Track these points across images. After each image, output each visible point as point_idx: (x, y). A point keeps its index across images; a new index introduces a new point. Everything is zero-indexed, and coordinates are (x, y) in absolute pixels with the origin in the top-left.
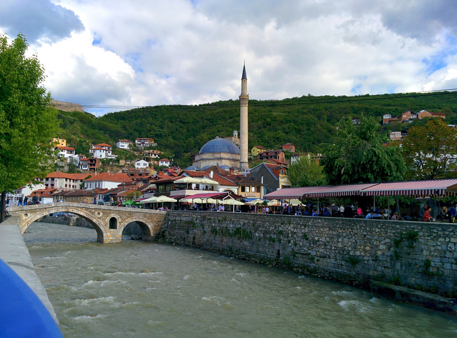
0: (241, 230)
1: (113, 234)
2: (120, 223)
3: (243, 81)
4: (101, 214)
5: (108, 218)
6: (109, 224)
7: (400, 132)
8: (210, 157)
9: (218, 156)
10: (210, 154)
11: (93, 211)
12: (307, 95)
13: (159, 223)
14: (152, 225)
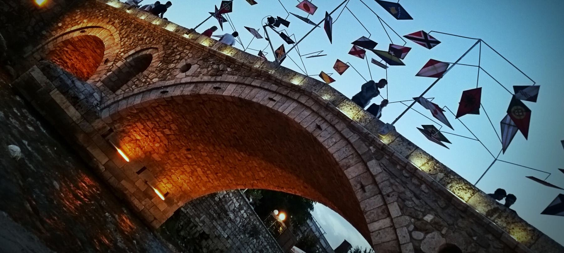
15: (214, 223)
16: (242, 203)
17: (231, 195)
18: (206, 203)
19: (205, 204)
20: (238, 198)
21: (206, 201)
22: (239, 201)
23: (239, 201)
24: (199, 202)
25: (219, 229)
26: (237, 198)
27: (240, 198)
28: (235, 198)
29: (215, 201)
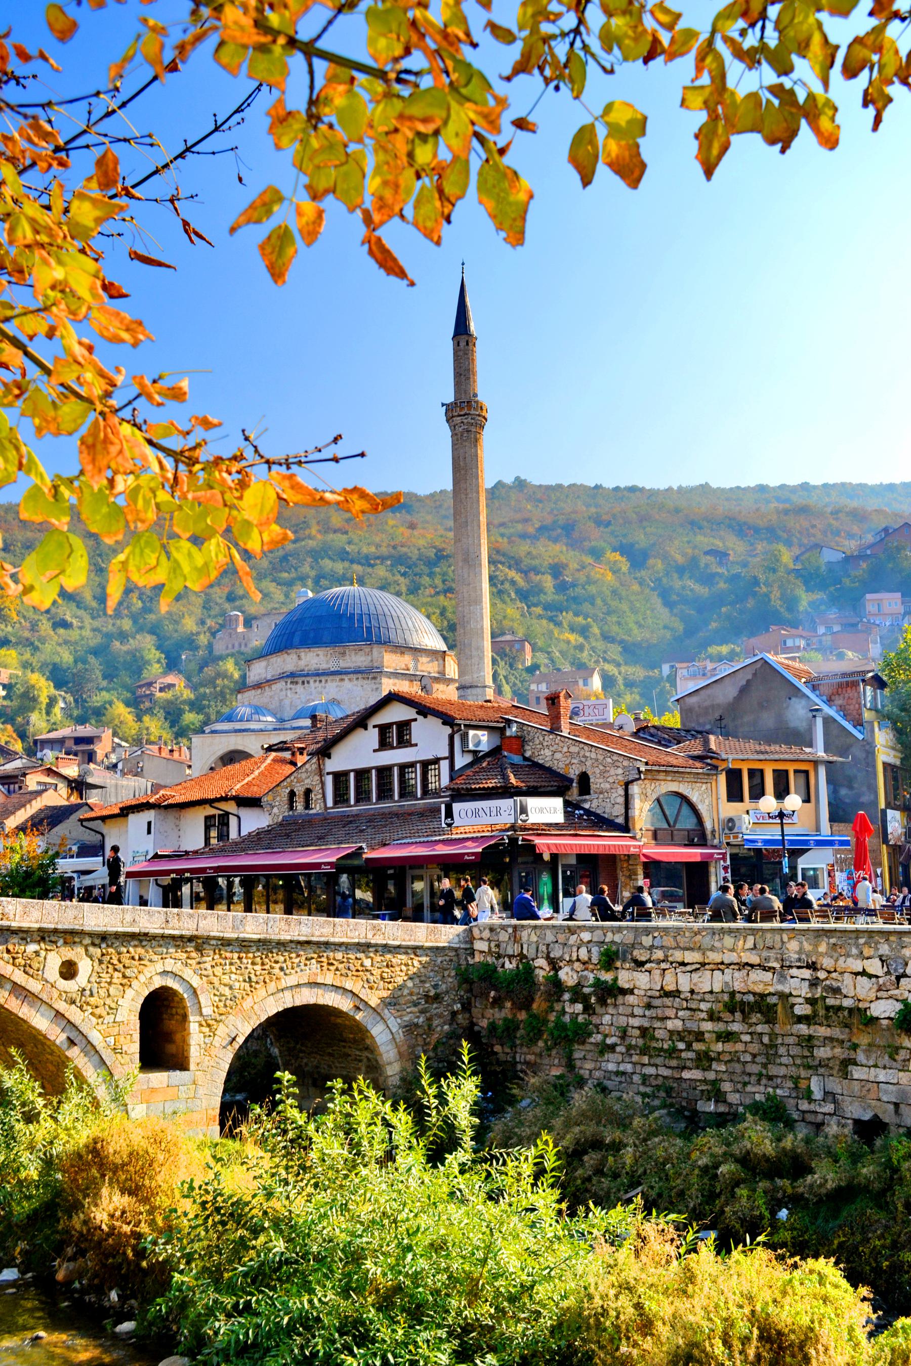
0: (587, 990)
1: (169, 1110)
2: (208, 1025)
3: (463, 344)
4: (85, 966)
5: (130, 993)
6: (137, 1036)
7: (899, 595)
8: (324, 666)
9: (356, 659)
10: (321, 652)
11: (32, 948)
12: (509, 480)
13: (435, 1009)
14: (394, 1024)
15: (855, 1077)
16: (884, 949)
17: (827, 963)
18: (782, 1044)
19: (782, 1050)
20: (857, 947)
21: (780, 1041)
22: (867, 952)
23: (867, 952)
24: (764, 1061)
25: (882, 1078)
26: (854, 951)
27: (862, 941)
28: (848, 955)
29: (800, 1019)
